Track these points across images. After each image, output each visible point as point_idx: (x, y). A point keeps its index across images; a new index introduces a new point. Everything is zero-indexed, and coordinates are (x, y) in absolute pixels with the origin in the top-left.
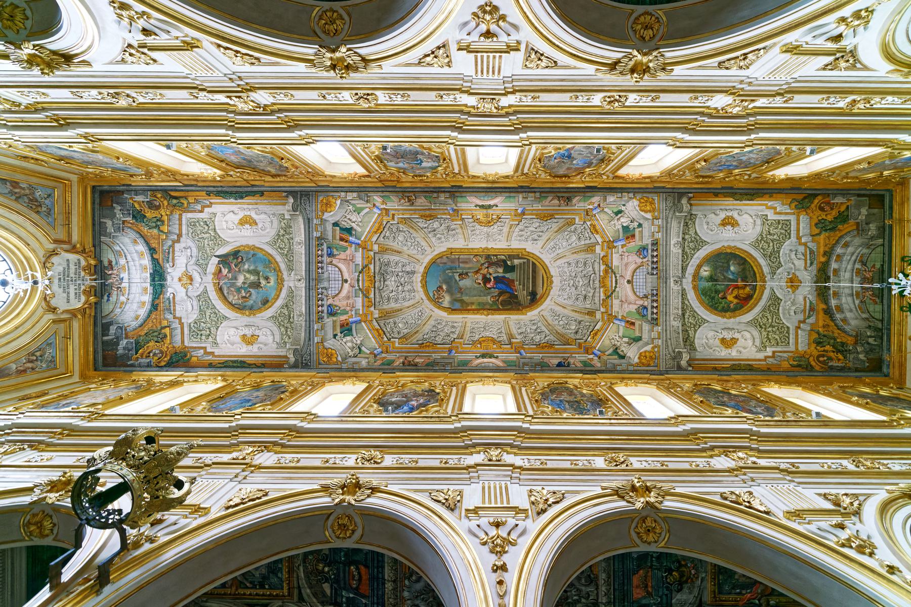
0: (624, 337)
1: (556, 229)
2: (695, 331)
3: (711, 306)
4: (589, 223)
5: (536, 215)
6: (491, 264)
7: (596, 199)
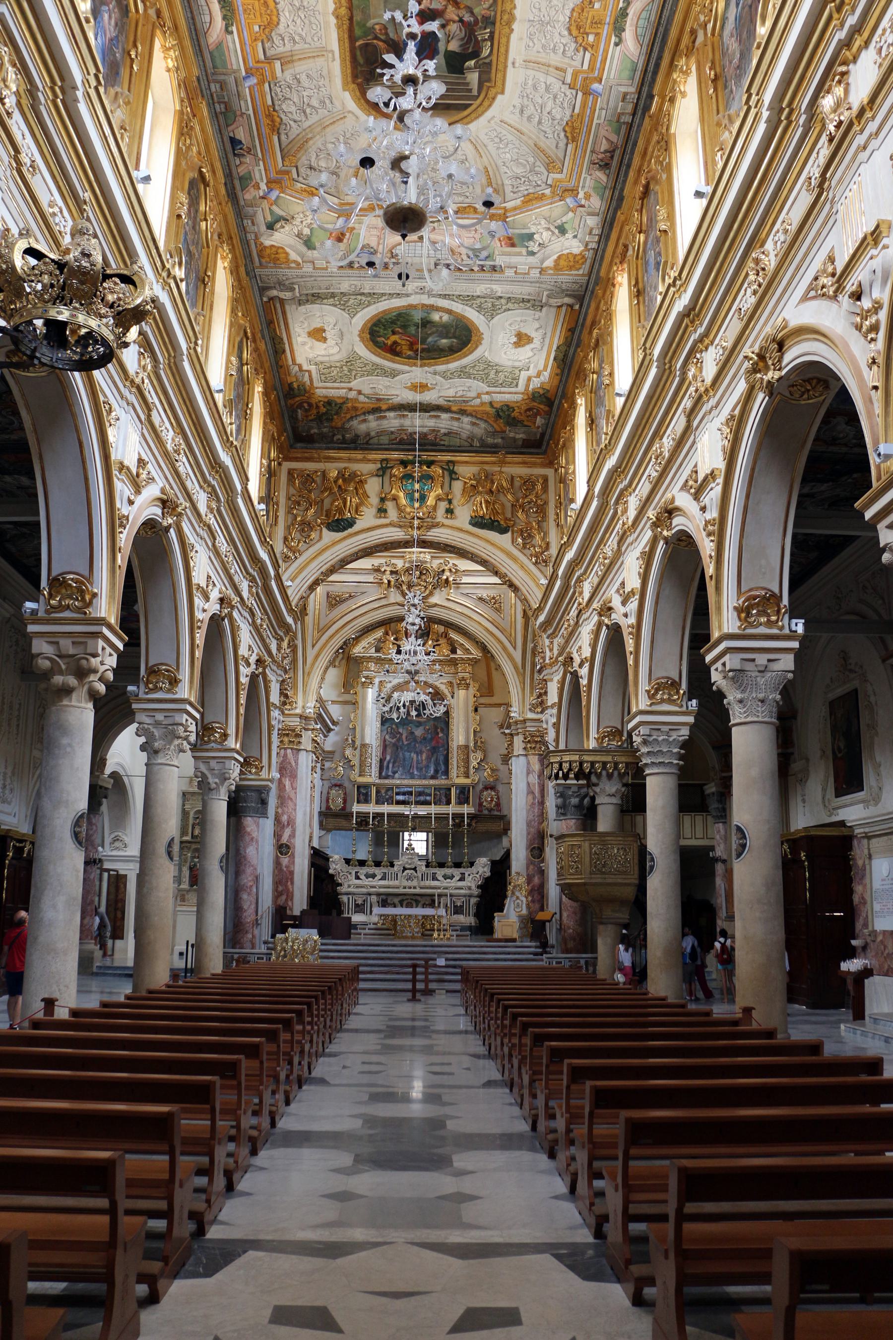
0: (311, 230)
1: (541, 144)
2: (335, 306)
3: (379, 321)
4: (548, 192)
5: (581, 115)
6: (470, 29)
7: (596, 203)
